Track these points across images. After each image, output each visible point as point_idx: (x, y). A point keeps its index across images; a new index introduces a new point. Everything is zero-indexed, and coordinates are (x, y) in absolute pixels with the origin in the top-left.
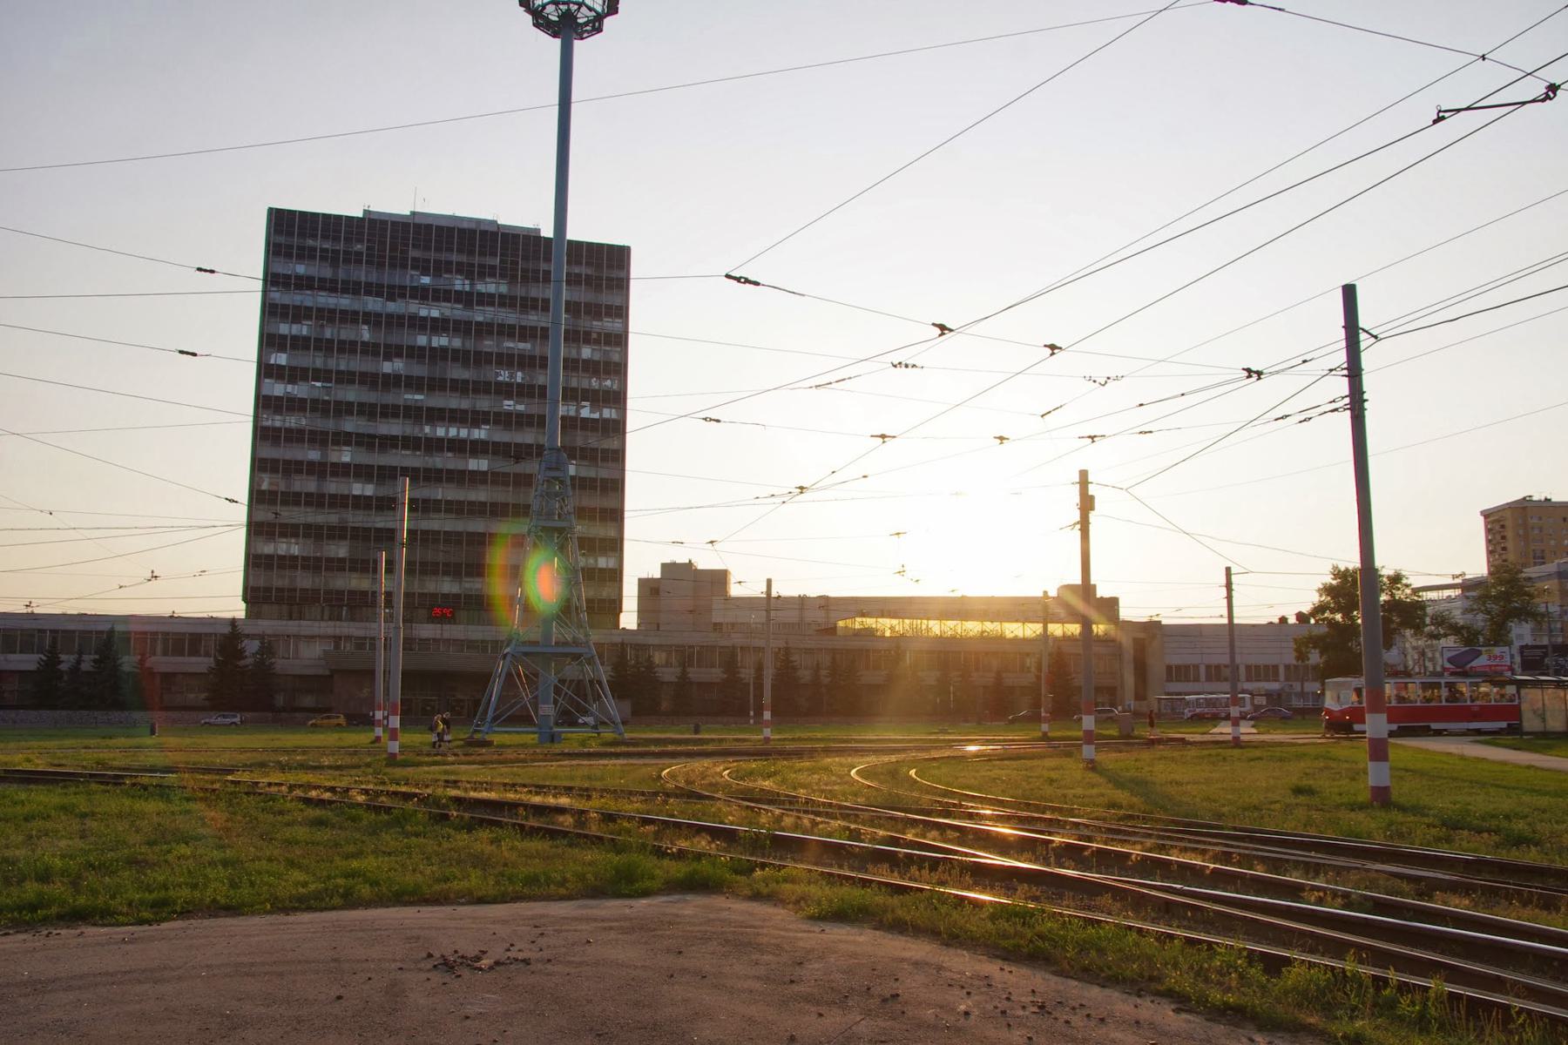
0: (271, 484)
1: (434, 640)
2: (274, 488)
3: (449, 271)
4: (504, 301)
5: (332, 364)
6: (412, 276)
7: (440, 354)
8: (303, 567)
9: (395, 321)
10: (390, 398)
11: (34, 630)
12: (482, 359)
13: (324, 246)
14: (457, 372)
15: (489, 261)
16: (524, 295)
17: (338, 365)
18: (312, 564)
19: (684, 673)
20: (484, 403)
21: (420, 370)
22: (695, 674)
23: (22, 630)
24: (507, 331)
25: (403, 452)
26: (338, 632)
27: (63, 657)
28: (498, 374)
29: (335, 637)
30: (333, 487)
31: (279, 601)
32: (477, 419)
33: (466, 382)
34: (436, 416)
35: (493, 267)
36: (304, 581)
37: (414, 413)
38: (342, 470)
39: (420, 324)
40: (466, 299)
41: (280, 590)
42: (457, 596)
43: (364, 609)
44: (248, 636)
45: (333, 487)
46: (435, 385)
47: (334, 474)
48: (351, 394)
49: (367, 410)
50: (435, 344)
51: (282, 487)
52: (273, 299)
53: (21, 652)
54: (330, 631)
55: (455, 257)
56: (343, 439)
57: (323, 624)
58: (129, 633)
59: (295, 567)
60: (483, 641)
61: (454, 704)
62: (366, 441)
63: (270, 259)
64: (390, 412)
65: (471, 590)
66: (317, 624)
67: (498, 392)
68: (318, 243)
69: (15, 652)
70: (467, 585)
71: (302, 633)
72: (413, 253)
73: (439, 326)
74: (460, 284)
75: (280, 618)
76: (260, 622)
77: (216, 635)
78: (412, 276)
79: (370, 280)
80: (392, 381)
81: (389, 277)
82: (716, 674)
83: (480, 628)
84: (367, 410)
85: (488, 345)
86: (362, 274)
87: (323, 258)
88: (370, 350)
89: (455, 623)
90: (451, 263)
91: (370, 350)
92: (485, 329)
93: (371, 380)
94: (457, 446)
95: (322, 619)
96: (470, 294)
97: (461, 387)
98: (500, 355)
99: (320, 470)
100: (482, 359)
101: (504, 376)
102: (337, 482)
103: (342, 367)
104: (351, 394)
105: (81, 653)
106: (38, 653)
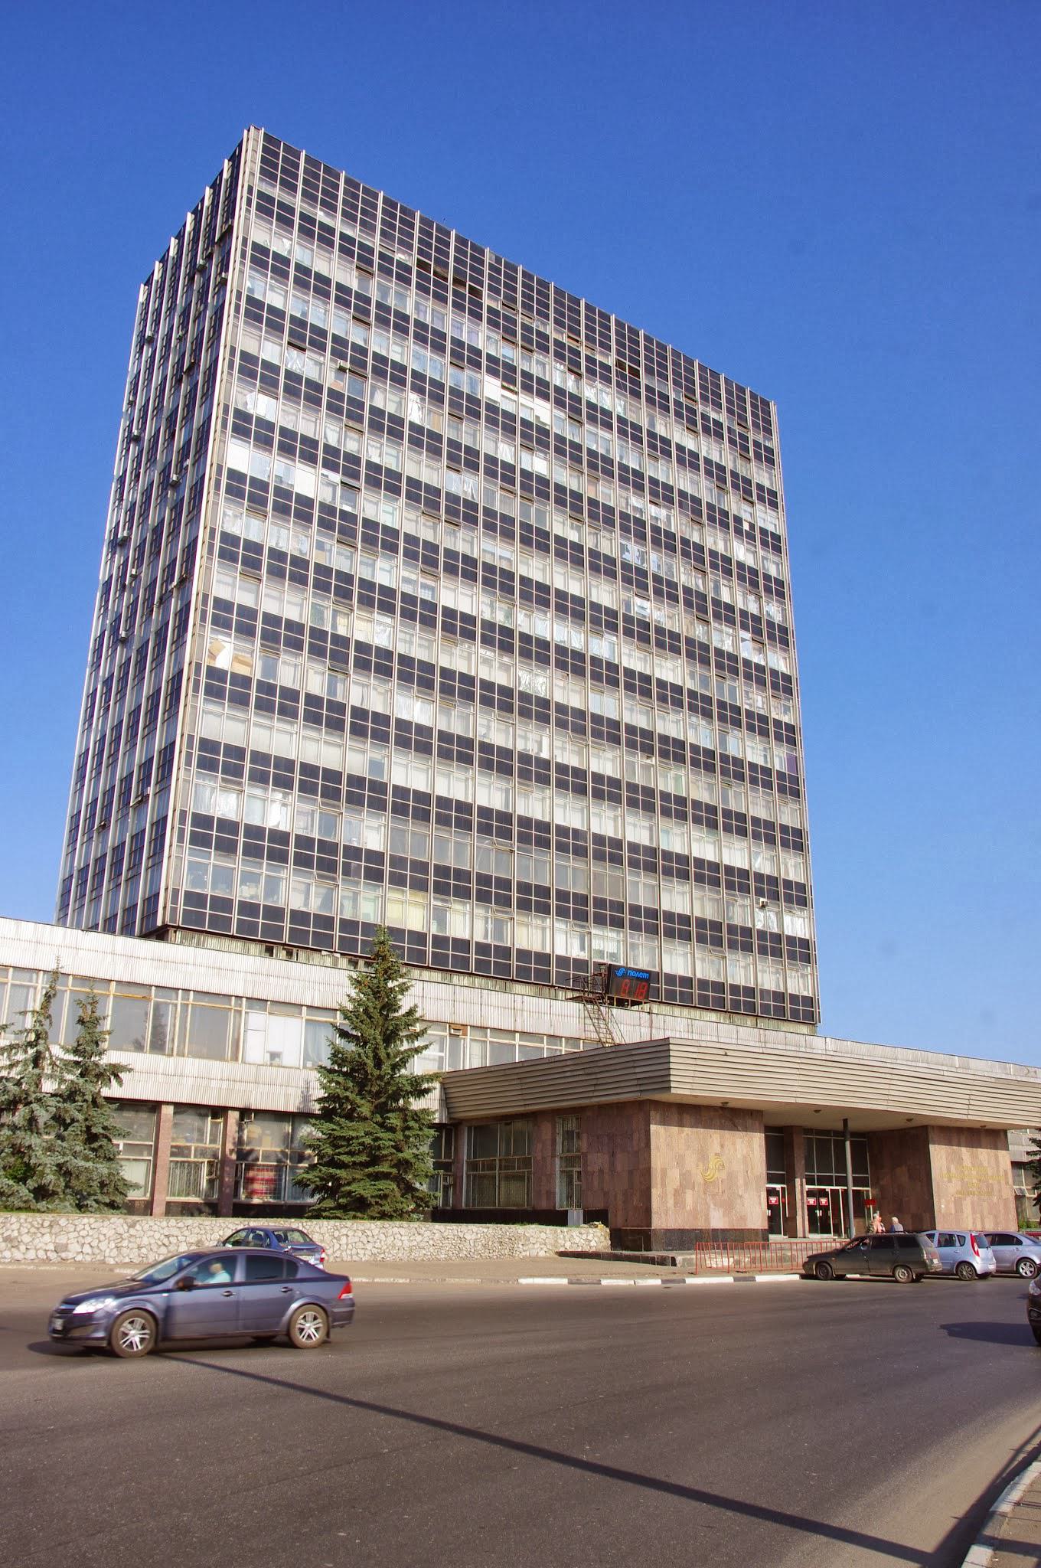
0: (236, 659)
2: (243, 670)
4: (630, 432)
8: (303, 861)
14: (560, 526)
28: (624, 549)
32: (605, 620)
34: (538, 595)
39: (504, 423)
41: (248, 908)
46: (537, 540)
47: (363, 665)
49: (423, 555)
64: (464, 568)
81: (452, 323)
84: (423, 555)
94: (572, 662)
97: (572, 554)
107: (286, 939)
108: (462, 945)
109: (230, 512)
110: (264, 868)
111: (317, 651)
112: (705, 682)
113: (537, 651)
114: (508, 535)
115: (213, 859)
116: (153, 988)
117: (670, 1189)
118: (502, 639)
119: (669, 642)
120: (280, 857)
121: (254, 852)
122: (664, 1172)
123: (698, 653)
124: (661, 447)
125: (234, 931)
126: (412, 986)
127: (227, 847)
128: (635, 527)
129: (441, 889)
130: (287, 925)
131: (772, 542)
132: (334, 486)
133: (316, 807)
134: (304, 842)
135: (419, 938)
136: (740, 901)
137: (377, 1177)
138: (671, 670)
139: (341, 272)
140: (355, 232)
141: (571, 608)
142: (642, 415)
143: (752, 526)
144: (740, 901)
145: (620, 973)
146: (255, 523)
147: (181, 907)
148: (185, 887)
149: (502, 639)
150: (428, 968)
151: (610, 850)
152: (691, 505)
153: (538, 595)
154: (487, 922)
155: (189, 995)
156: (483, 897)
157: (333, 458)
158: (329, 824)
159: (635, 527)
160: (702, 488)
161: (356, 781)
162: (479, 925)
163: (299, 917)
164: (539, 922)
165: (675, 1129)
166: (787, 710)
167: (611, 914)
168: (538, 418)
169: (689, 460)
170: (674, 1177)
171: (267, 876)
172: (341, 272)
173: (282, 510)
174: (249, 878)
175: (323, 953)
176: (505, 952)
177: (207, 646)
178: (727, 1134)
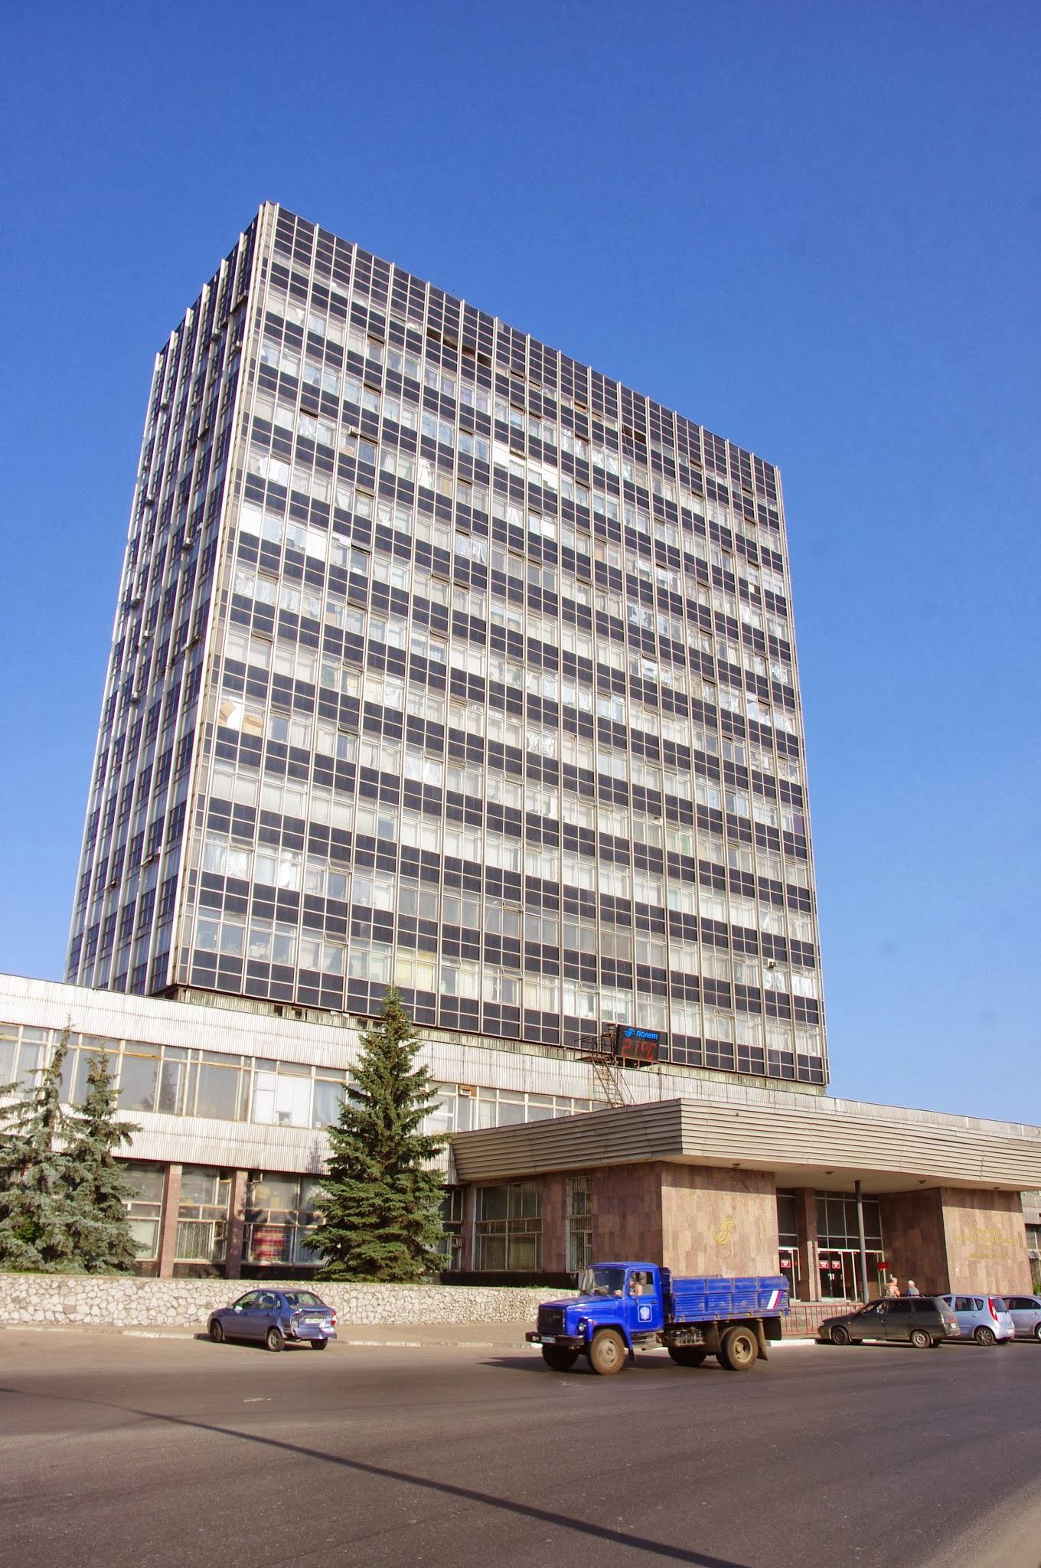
0: (247, 719)
2: (253, 731)
4: (636, 496)
8: (312, 921)
14: (567, 588)
28: (631, 611)
32: (612, 682)
34: (546, 657)
39: (512, 487)
41: (258, 968)
46: (545, 603)
47: (372, 726)
49: (433, 618)
56: (389, 661)
64: (473, 630)
81: (461, 390)
84: (433, 618)
94: (580, 724)
97: (580, 617)
107: (295, 999)
108: (471, 1005)
109: (242, 575)
110: (274, 928)
111: (327, 713)
112: (712, 743)
113: (544, 712)
114: (516, 598)
115: (223, 919)
116: (163, 1047)
117: (682, 1253)
118: (510, 700)
119: (675, 704)
120: (288, 916)
121: (262, 911)
122: (676, 1236)
123: (705, 714)
124: (667, 511)
125: (243, 991)
126: (423, 1045)
127: (237, 907)
128: (641, 590)
129: (450, 950)
130: (296, 985)
131: (777, 605)
132: (345, 549)
133: (325, 867)
134: (314, 902)
135: (428, 998)
136: (748, 962)
137: (387, 1239)
138: (678, 731)
139: (352, 340)
141: (579, 670)
142: (648, 480)
143: (757, 589)
144: (748, 962)
145: (629, 1034)
146: (267, 585)
147: (191, 966)
148: (195, 946)
149: (510, 700)
150: (436, 1028)
151: (618, 911)
152: (698, 568)
153: (546, 657)
154: (495, 983)
155: (198, 1054)
156: (492, 958)
157: (343, 522)
158: (338, 885)
159: (641, 590)
160: (708, 552)
161: (365, 842)
162: (488, 985)
163: (309, 977)
164: (547, 983)
165: (686, 1191)
166: (793, 771)
168: (545, 483)
169: (695, 524)
170: (686, 1239)
171: (276, 936)
172: (352, 340)
173: (293, 573)
174: (259, 938)
175: (332, 1013)
176: (514, 1013)
177: (219, 706)
178: (738, 1195)
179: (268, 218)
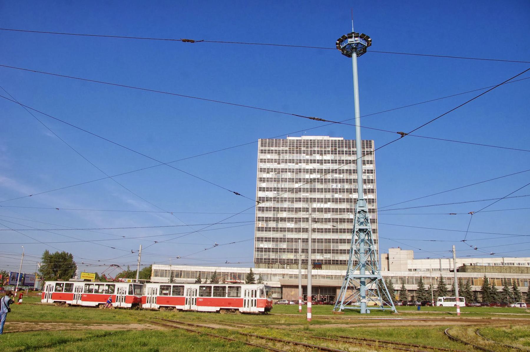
0: (262, 225)
1: (315, 275)
2: (263, 226)
3: (315, 153)
4: (334, 162)
5: (279, 186)
6: (303, 156)
7: (313, 181)
8: (272, 251)
9: (300, 171)
10: (298, 195)
11: (194, 271)
12: (327, 181)
13: (276, 149)
14: (318, 186)
15: (327, 149)
16: (339, 159)
17: (281, 186)
18: (275, 250)
19: (403, 286)
20: (329, 196)
21: (308, 186)
22: (408, 287)
23: (191, 271)
24: (334, 171)
25: (303, 213)
26: (284, 273)
27: (202, 280)
28: (332, 186)
29: (283, 274)
30: (281, 225)
31: (265, 263)
32: (327, 200)
33: (322, 189)
34: (313, 200)
35: (329, 151)
36: (272, 256)
37: (306, 200)
38: (283, 220)
39: (307, 171)
40: (321, 162)
42: (322, 260)
43: (292, 265)
44: (255, 274)
45: (281, 225)
46: (313, 190)
48: (286, 195)
49: (292, 200)
50: (311, 178)
51: (265, 226)
52: (261, 167)
53: (191, 278)
54: (281, 273)
55: (316, 149)
56: (284, 210)
57: (279, 270)
58: (220, 272)
59: (270, 251)
60: (331, 276)
61: (322, 297)
62: (290, 210)
63: (260, 155)
64: (299, 200)
65: (327, 258)
66: (277, 270)
67: (333, 192)
68: (273, 148)
69: (189, 278)
70: (325, 257)
71: (272, 273)
72: (303, 149)
73: (313, 171)
74: (318, 157)
75: (265, 268)
76: (259, 269)
77: (246, 273)
78: (303, 156)
79: (290, 159)
80: (299, 190)
81: (295, 156)
82: (415, 287)
83: (330, 271)
84: (292, 200)
85: (329, 176)
86: (287, 156)
87: (276, 153)
88: (292, 180)
89: (321, 269)
90: (315, 151)
91: (292, 180)
92: (327, 171)
93: (291, 190)
95: (279, 268)
96: (322, 160)
97: (320, 190)
98: (333, 179)
99: (276, 220)
100: (327, 181)
101: (334, 186)
102: (282, 224)
103: (283, 187)
104: (286, 195)
105: (207, 279)
106: (195, 278)
110: (267, 253)
111: (274, 221)
112: (351, 206)
114: (307, 191)
115: (260, 253)
117: (285, 296)
119: (341, 201)
120: (269, 251)
124: (341, 162)
127: (261, 251)
128: (335, 181)
133: (275, 243)
134: (273, 249)
135: (292, 260)
138: (344, 206)
140: (277, 149)
141: (320, 200)
142: (338, 157)
143: (365, 170)
147: (256, 260)
148: (256, 257)
151: (328, 241)
153: (313, 200)
159: (335, 181)
161: (281, 238)
165: (287, 289)
167: (328, 251)
168: (313, 167)
172: (275, 156)
173: (267, 200)
179: (260, 140)
